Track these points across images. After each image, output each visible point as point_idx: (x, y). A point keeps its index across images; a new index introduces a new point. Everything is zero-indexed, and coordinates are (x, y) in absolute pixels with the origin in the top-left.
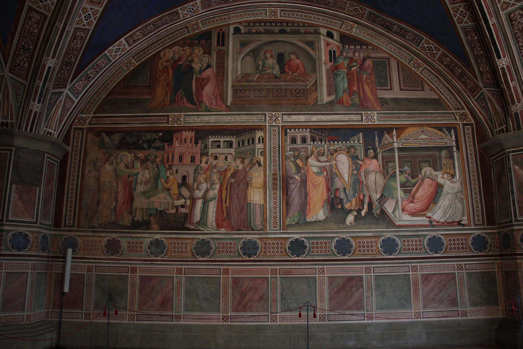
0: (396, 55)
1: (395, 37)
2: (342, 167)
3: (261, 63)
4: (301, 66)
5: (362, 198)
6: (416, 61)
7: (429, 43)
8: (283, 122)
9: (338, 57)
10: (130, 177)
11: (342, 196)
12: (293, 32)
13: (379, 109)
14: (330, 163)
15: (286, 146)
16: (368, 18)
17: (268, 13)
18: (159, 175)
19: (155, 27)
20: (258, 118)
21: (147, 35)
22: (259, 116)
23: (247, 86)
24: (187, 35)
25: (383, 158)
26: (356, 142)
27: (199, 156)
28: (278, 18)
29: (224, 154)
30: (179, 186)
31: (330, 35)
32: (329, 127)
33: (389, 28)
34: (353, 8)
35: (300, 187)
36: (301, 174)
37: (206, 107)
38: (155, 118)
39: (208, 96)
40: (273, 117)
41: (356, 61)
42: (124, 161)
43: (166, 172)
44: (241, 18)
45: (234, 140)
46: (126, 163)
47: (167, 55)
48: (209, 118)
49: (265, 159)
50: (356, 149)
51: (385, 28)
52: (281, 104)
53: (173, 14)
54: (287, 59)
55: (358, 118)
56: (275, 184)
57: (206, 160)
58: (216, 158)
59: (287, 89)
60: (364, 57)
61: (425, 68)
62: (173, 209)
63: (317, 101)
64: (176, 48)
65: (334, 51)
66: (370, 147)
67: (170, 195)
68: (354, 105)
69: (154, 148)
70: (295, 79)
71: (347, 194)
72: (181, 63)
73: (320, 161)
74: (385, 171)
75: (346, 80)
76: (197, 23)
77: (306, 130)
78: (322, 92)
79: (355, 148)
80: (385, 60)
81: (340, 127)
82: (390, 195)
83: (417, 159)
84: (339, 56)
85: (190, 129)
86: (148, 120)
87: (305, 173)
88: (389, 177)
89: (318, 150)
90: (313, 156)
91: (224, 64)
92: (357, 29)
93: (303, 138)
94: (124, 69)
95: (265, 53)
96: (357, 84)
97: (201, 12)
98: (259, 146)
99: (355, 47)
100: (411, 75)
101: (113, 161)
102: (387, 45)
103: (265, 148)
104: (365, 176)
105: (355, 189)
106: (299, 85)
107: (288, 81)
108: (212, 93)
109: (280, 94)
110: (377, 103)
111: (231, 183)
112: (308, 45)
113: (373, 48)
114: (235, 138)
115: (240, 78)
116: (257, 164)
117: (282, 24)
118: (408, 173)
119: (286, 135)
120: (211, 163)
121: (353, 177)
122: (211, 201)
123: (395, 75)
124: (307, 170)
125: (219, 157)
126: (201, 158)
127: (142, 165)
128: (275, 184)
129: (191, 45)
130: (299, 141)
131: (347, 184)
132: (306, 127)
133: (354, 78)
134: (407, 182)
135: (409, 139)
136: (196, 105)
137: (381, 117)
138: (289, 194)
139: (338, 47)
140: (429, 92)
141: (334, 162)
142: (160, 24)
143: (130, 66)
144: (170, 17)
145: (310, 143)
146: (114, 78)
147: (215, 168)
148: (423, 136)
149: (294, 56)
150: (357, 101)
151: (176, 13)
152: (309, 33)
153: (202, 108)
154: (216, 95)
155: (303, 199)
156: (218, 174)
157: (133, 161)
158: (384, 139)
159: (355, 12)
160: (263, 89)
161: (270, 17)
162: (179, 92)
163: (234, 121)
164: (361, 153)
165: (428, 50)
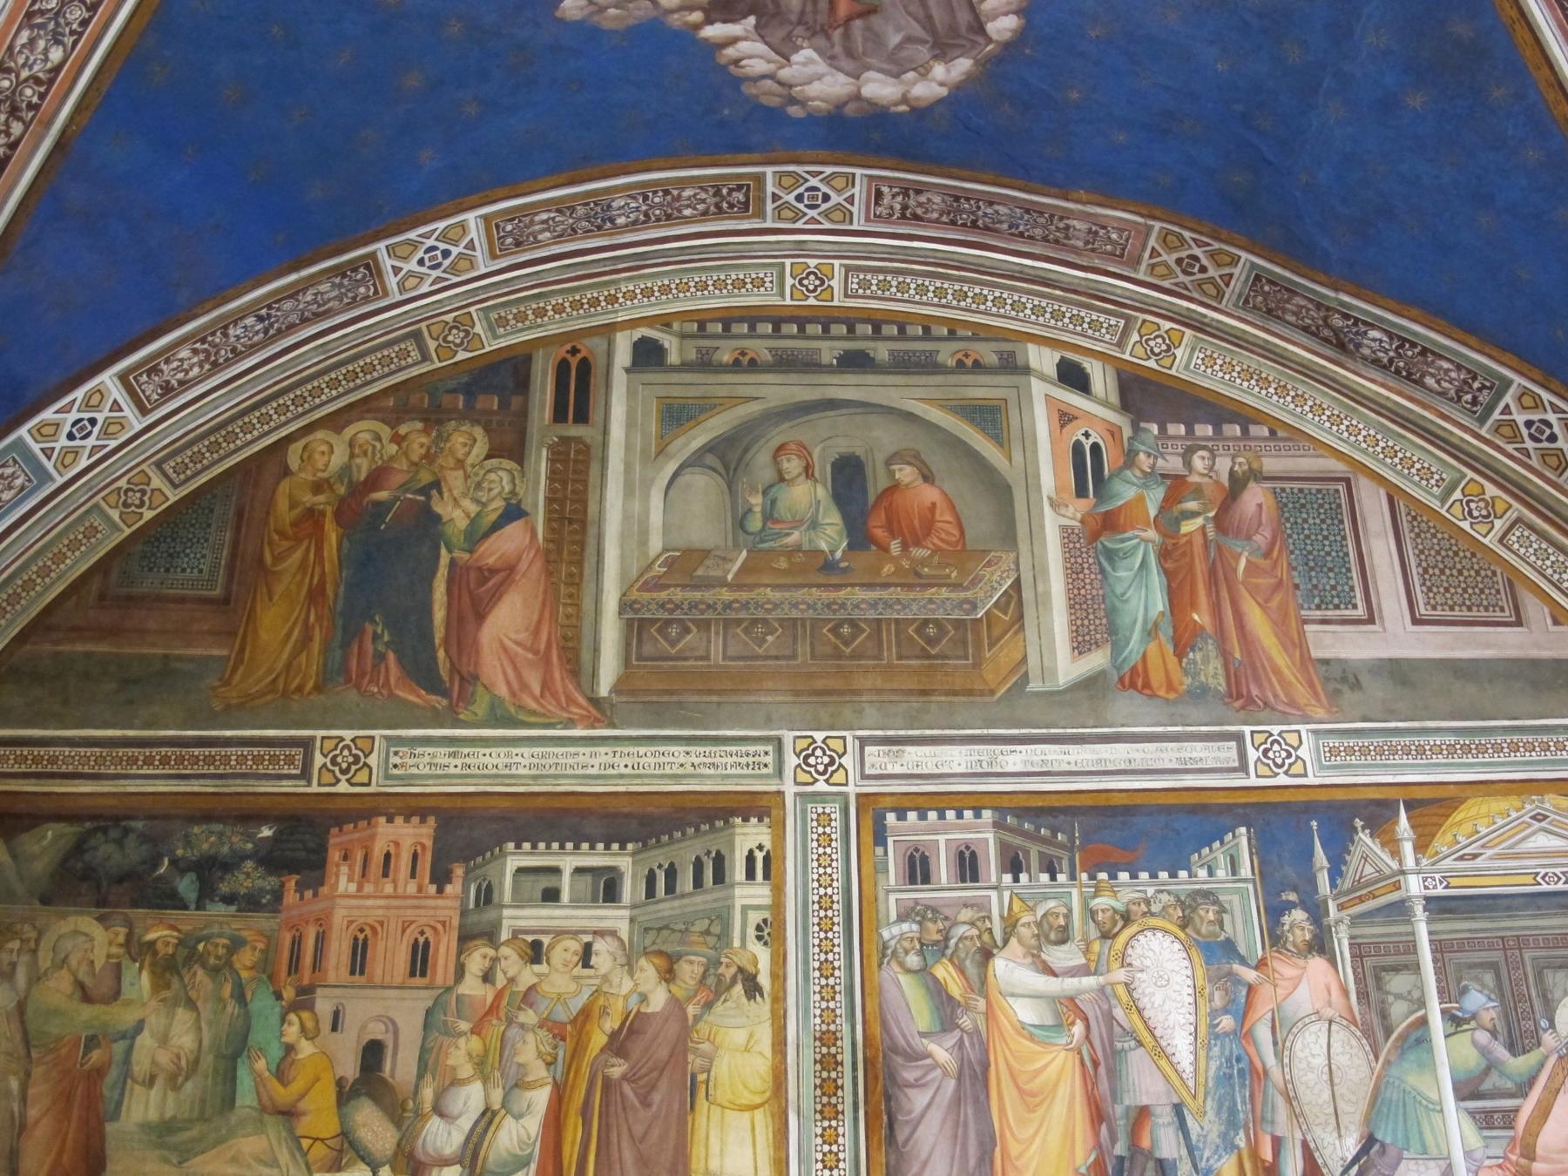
0: (1382, 462)
1: (1373, 381)
2: (1158, 999)
3: (756, 501)
4: (944, 515)
5: (1267, 1154)
6: (1473, 489)
7: (1538, 404)
8: (864, 777)
9: (1111, 476)
10: (98, 1045)
11: (1168, 1145)
12: (904, 365)
13: (1320, 713)
14: (1101, 979)
15: (881, 895)
16: (1246, 301)
17: (789, 281)
18: (246, 1036)
19: (266, 331)
20: (744, 760)
21: (229, 363)
22: (752, 749)
23: (694, 605)
24: (415, 371)
25: (1359, 952)
26: (1221, 873)
27: (454, 944)
28: (836, 303)
29: (576, 933)
30: (346, 1095)
31: (1072, 376)
32: (1087, 801)
33: (1342, 345)
34: (1175, 256)
35: (957, 1101)
36: (957, 1033)
37: (495, 703)
38: (246, 751)
39: (505, 649)
40: (819, 752)
41: (1198, 492)
42: (73, 961)
43: (283, 1020)
44: (668, 301)
45: (624, 863)
46: (82, 976)
47: (317, 456)
48: (507, 755)
49: (779, 960)
50: (1222, 910)
51: (1326, 340)
52: (854, 692)
53: (355, 270)
54: (877, 482)
55: (1223, 755)
56: (827, 1088)
57: (487, 963)
58: (536, 953)
59: (879, 621)
60: (1232, 473)
61: (1518, 520)
63: (1025, 678)
64: (363, 429)
65: (1095, 448)
66: (1293, 897)
67: (297, 1140)
68: (1200, 694)
69: (229, 899)
70: (918, 575)
71: (1194, 1138)
72: (382, 495)
73: (1049, 971)
74: (1376, 1021)
75: (1156, 580)
76: (466, 320)
77: (978, 815)
78: (1044, 632)
79: (1216, 902)
80: (1332, 486)
81: (1138, 800)
82: (1407, 1139)
83: (1527, 955)
84: (1121, 469)
85: (414, 808)
86: (209, 760)
87: (978, 1032)
88: (1395, 1047)
89: (1040, 913)
90: (1013, 941)
91: (584, 503)
92: (1193, 349)
93: (961, 854)
94: (108, 519)
95: (775, 457)
96: (1209, 594)
97: (483, 270)
98: (750, 895)
99: (1190, 431)
100: (1456, 554)
101: (13, 965)
102: (1335, 420)
103: (778, 906)
104: (1275, 1043)
105: (1233, 1112)
106: (940, 603)
107: (885, 586)
108: (523, 636)
109: (847, 644)
110: (1311, 685)
111: (608, 1084)
112: (972, 421)
113: (1273, 432)
114: (634, 854)
115: (658, 569)
116: (739, 989)
117: (851, 330)
118: (1489, 1026)
119: (880, 838)
120: (512, 981)
121: (1216, 1050)
123: (1382, 552)
124: (989, 1014)
125: (552, 946)
126: (460, 953)
127: (159, 984)
128: (829, 1087)
129: (435, 418)
130: (943, 869)
131: (1191, 1083)
132: (977, 803)
133: (1191, 567)
134: (1487, 1071)
135: (1475, 856)
136: (445, 693)
137: (1334, 752)
138: (901, 1137)
139: (1114, 432)
140: (1552, 628)
141: (1120, 975)
142: (294, 318)
143: (142, 504)
144: (341, 285)
145: (1000, 879)
146: (59, 558)
147: (531, 1006)
148: (1542, 841)
149: (908, 469)
150: (1212, 672)
151: (367, 267)
152: (978, 367)
153: (474, 708)
154: (542, 646)
155: (972, 1162)
156: (542, 1033)
157: (119, 966)
158: (1357, 855)
159: (1185, 272)
160: (765, 621)
161: (797, 295)
162: (369, 628)
163: (629, 771)
164: (1246, 929)
165: (1532, 437)
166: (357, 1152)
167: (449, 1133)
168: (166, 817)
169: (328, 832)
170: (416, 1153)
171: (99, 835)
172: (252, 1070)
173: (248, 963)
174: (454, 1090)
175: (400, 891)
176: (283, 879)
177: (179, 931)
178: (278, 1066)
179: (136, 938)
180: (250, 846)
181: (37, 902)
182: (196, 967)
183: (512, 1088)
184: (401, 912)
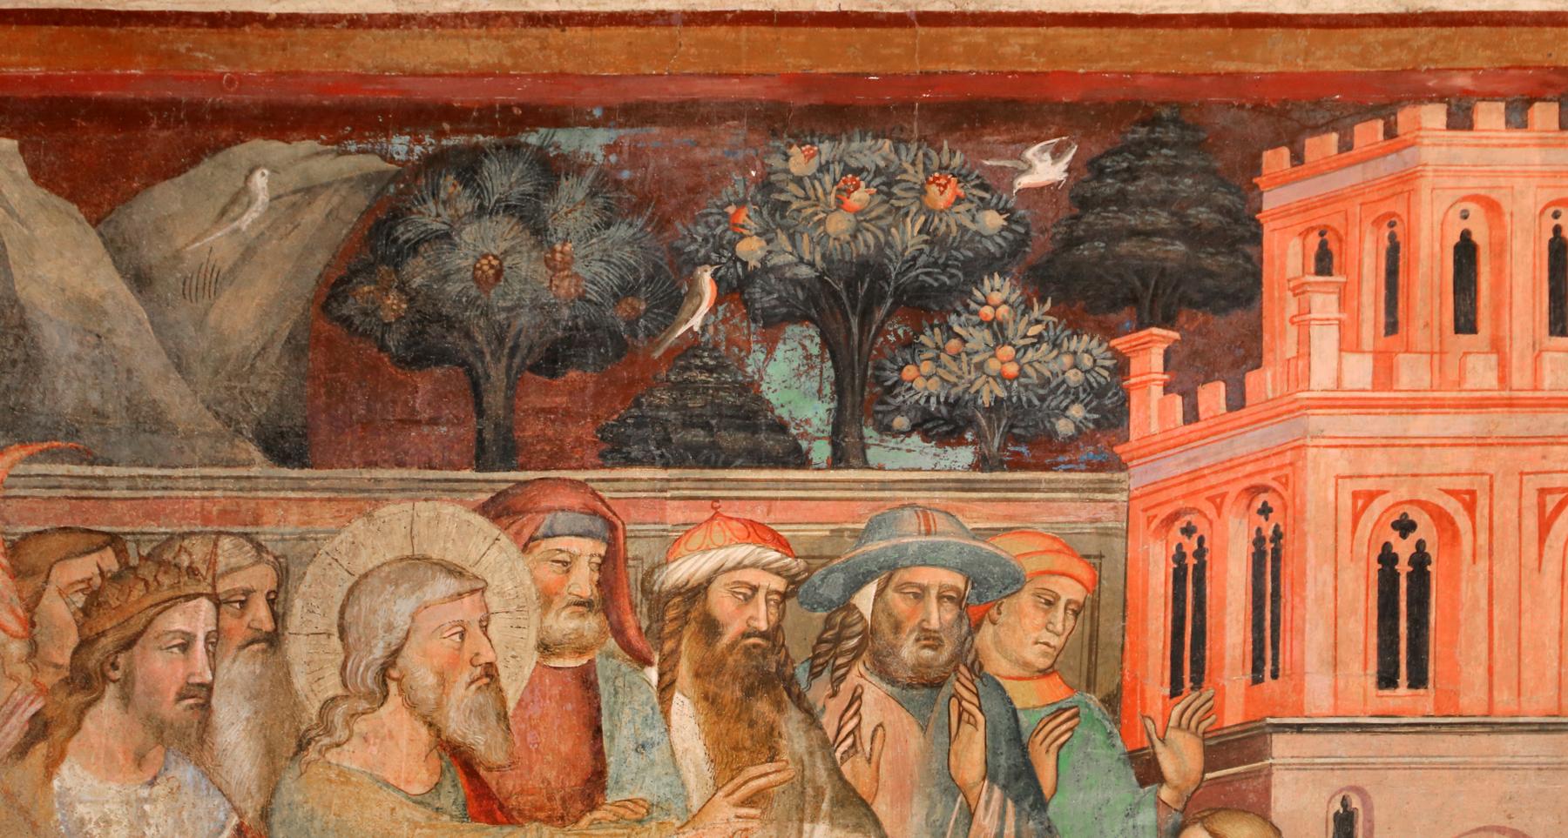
42: (420, 670)
46: (457, 725)
101: (201, 696)
157: (586, 680)
168: (685, 114)
169: (1255, 167)
171: (449, 184)
173: (1036, 656)
175: (1520, 379)
176: (1120, 343)
177: (782, 544)
179: (634, 574)
180: (992, 221)
181: (258, 455)
182: (859, 675)
184: (1528, 457)
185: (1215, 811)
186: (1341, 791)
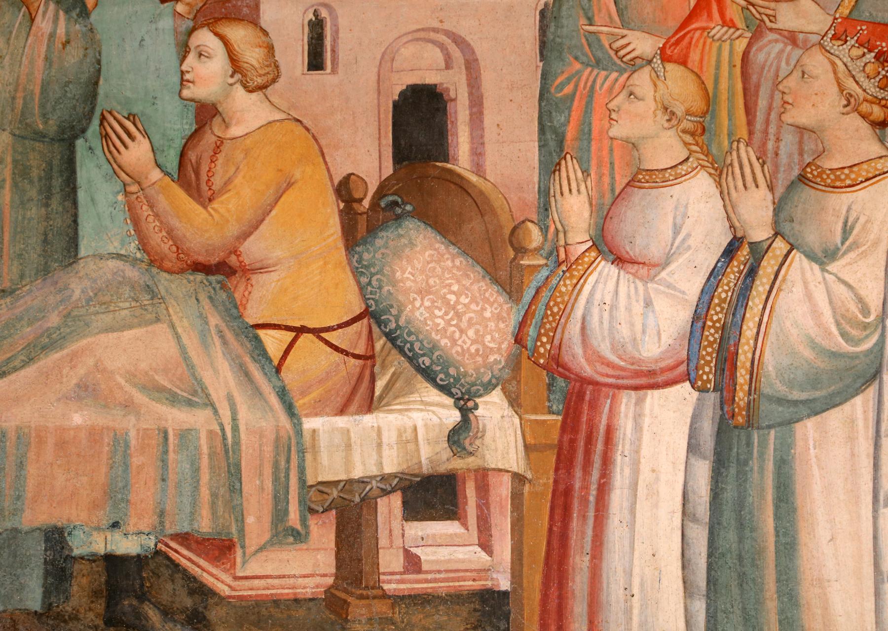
18: (97, 84)
43: (184, 50)
62: (299, 536)
122: (817, 408)
156: (848, 51)
166: (412, 360)
167: (648, 304)
170: (566, 358)
172: (117, 169)
174: (637, 195)
178: (183, 155)
183: (791, 187)
185: (217, 20)
186: (313, 6)
